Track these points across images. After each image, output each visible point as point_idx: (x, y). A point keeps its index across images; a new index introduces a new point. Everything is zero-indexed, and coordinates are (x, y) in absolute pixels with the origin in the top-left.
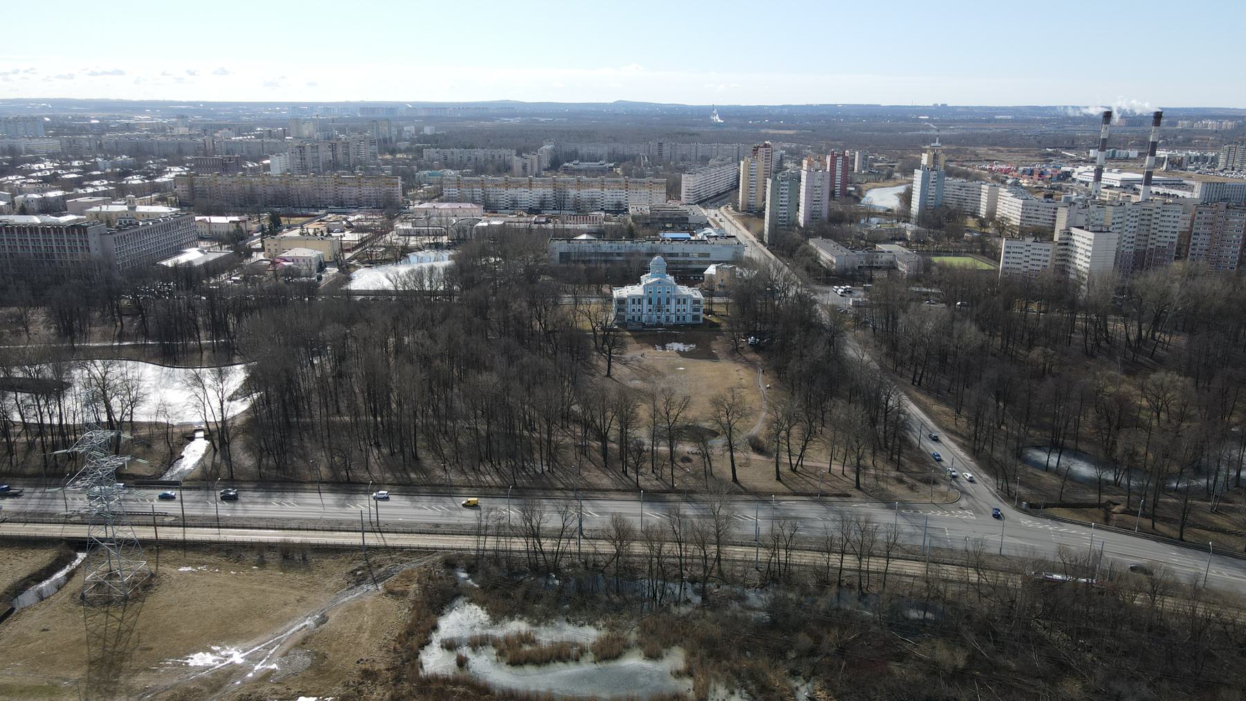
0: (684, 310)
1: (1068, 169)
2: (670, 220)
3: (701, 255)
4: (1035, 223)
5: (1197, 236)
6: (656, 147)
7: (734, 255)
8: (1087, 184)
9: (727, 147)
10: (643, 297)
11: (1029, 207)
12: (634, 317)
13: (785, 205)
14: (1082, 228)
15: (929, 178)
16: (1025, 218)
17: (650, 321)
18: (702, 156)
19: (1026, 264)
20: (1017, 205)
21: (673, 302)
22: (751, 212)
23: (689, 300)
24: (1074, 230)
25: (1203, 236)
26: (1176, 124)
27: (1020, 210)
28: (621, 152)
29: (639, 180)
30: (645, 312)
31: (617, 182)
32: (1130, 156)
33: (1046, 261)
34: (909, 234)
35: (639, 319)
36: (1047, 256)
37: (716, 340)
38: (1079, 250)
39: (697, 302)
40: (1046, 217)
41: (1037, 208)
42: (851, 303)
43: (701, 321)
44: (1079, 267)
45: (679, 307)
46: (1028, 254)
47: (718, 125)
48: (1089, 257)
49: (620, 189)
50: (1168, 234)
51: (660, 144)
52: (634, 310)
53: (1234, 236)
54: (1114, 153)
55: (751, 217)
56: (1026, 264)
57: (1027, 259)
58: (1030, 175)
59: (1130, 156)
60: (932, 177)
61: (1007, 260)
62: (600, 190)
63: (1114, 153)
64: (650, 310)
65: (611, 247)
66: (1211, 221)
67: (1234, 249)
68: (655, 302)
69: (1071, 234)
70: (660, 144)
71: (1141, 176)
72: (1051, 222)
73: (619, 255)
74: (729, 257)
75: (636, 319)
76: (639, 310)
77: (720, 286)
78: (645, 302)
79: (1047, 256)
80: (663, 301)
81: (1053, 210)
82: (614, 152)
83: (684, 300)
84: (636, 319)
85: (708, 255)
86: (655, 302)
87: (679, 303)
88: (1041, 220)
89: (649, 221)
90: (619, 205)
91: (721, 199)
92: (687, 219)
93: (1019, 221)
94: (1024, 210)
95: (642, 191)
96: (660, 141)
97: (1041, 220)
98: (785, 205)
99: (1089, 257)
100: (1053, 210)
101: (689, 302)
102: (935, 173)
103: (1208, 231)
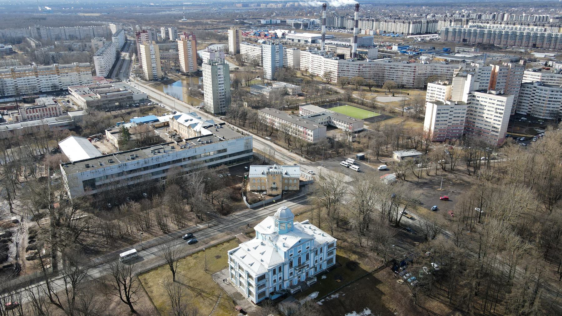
0: (321, 258)
1: (273, 32)
2: (116, 100)
3: (219, 152)
4: (347, 74)
5: (499, 84)
6: (36, 31)
7: (245, 146)
8: (293, 40)
9: (85, 28)
10: (284, 264)
11: (343, 65)
12: (275, 288)
13: (223, 84)
14: (485, 91)
15: (275, 50)
16: (340, 71)
17: (292, 286)
18: (70, 35)
19: (450, 121)
20: (333, 63)
21: (312, 256)
22: (157, 80)
23: (326, 247)
24: (477, 94)
25: (501, 84)
26: (260, 6)
27: (337, 67)
28: (9, 36)
29: (67, 65)
30: (286, 277)
31: (48, 69)
32: (278, 22)
33: (463, 117)
34: (290, 91)
35: (280, 286)
36: (464, 113)
37: (382, 293)
38: (485, 108)
39: (330, 246)
40: (355, 70)
41: (348, 65)
42: (386, 182)
43: (334, 262)
44: (487, 120)
45: (318, 258)
46: (451, 113)
47: (49, 11)
48: (501, 113)
49: (52, 74)
50: (484, 84)
51: (38, 29)
52: (275, 281)
53: (517, 82)
54: (271, 21)
55: (159, 85)
56: (450, 121)
57: (451, 117)
58: (259, 36)
59: (278, 22)
60: (276, 49)
61: (438, 119)
62: (34, 77)
63: (271, 21)
64: (291, 274)
65: (138, 163)
66: (506, 75)
67: (517, 90)
68: (295, 264)
69: (474, 96)
70: (38, 29)
71: (320, 35)
72: (357, 73)
73: (146, 169)
74: (242, 149)
75: (277, 289)
76: (280, 278)
77: (272, 189)
78: (287, 267)
79: (464, 113)
80: (303, 260)
81: (358, 66)
82: (3, 36)
83: (321, 249)
84: (277, 289)
85: (225, 150)
86: (295, 264)
87: (316, 254)
88: (352, 72)
89: (100, 104)
90: (54, 86)
91: (120, 68)
92: (132, 97)
93: (337, 73)
94: (339, 67)
95: (71, 74)
96: (38, 26)
97: (351, 72)
98: (223, 84)
99: (501, 113)
100: (358, 66)
101: (325, 249)
102: (278, 46)
103: (504, 81)
